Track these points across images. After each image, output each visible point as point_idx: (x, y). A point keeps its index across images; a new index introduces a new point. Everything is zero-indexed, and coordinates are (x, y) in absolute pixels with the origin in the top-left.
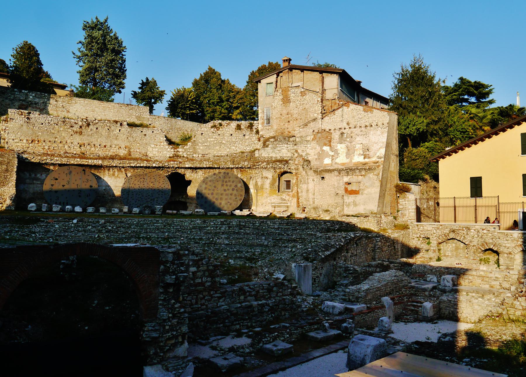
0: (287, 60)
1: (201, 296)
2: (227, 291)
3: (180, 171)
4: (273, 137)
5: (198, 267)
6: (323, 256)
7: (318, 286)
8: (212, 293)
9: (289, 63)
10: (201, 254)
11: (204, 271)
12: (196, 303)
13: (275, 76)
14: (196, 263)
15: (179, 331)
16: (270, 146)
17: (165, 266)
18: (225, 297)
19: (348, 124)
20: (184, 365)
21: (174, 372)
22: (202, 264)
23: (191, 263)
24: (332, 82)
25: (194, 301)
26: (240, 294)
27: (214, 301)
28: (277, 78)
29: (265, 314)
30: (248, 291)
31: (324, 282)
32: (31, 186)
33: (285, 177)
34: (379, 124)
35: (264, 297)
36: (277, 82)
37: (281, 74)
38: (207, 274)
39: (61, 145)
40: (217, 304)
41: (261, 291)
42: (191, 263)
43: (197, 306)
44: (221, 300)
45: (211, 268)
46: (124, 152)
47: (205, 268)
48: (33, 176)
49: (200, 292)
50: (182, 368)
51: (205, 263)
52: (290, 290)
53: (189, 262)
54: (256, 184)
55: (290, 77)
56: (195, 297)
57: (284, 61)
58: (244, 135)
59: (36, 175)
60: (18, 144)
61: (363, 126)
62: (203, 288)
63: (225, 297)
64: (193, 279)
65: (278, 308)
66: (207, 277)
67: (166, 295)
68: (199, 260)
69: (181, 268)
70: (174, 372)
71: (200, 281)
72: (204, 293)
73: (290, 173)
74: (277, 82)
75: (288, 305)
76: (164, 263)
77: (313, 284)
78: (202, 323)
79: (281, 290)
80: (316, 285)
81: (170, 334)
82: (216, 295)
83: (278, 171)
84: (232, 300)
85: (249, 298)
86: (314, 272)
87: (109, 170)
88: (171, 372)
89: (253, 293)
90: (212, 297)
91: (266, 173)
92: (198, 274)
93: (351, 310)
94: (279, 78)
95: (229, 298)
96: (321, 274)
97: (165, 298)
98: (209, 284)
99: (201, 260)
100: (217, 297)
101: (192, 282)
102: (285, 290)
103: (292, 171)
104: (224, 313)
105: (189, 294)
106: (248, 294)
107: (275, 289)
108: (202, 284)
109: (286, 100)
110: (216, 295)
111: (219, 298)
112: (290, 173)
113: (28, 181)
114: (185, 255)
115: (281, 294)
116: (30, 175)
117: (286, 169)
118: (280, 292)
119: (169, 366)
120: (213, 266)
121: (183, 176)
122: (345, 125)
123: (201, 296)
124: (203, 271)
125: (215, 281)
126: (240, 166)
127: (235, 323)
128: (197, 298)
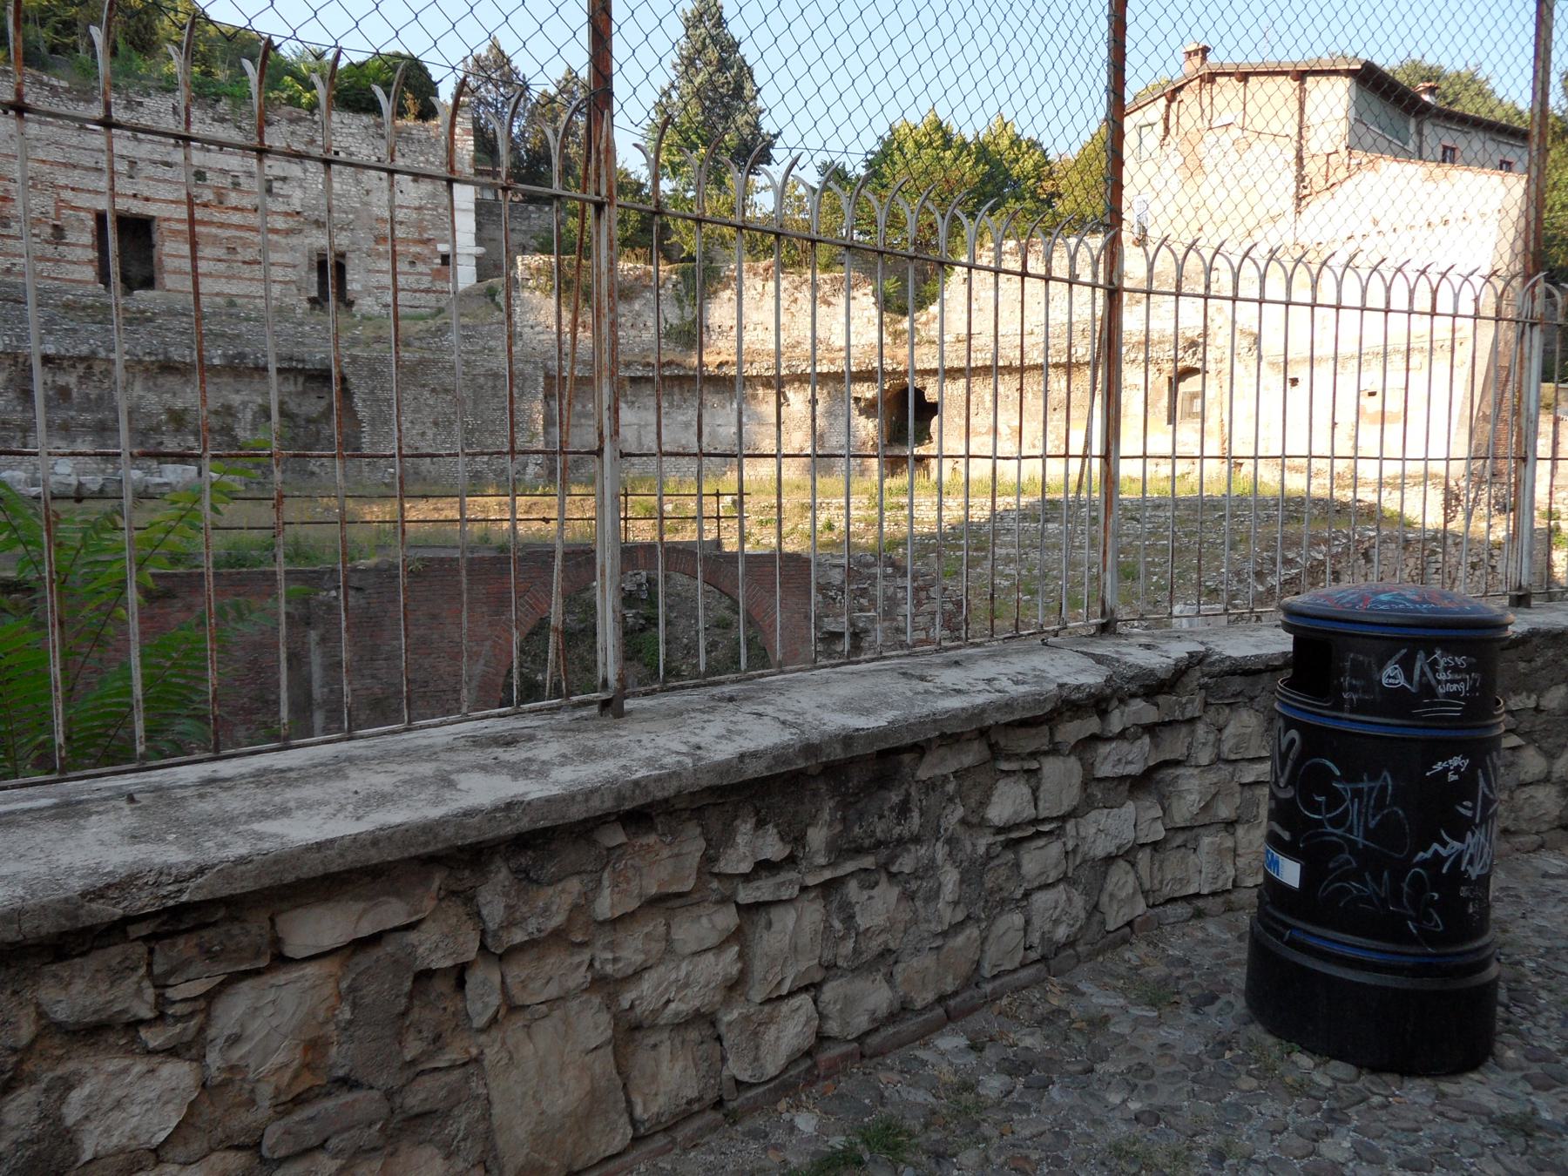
0: (1196, 52)
6: (1260, 588)
9: (1204, 58)
10: (923, 575)
13: (1163, 102)
19: (1376, 223)
22: (928, 598)
24: (1333, 100)
28: (1168, 107)
33: (1190, 385)
34: (1471, 214)
36: (1167, 119)
39: (633, 333)
48: (579, 407)
53: (895, 593)
55: (1206, 100)
57: (1189, 54)
60: (542, 337)
61: (1421, 220)
94: (1174, 106)
109: (1194, 168)
122: (1368, 227)
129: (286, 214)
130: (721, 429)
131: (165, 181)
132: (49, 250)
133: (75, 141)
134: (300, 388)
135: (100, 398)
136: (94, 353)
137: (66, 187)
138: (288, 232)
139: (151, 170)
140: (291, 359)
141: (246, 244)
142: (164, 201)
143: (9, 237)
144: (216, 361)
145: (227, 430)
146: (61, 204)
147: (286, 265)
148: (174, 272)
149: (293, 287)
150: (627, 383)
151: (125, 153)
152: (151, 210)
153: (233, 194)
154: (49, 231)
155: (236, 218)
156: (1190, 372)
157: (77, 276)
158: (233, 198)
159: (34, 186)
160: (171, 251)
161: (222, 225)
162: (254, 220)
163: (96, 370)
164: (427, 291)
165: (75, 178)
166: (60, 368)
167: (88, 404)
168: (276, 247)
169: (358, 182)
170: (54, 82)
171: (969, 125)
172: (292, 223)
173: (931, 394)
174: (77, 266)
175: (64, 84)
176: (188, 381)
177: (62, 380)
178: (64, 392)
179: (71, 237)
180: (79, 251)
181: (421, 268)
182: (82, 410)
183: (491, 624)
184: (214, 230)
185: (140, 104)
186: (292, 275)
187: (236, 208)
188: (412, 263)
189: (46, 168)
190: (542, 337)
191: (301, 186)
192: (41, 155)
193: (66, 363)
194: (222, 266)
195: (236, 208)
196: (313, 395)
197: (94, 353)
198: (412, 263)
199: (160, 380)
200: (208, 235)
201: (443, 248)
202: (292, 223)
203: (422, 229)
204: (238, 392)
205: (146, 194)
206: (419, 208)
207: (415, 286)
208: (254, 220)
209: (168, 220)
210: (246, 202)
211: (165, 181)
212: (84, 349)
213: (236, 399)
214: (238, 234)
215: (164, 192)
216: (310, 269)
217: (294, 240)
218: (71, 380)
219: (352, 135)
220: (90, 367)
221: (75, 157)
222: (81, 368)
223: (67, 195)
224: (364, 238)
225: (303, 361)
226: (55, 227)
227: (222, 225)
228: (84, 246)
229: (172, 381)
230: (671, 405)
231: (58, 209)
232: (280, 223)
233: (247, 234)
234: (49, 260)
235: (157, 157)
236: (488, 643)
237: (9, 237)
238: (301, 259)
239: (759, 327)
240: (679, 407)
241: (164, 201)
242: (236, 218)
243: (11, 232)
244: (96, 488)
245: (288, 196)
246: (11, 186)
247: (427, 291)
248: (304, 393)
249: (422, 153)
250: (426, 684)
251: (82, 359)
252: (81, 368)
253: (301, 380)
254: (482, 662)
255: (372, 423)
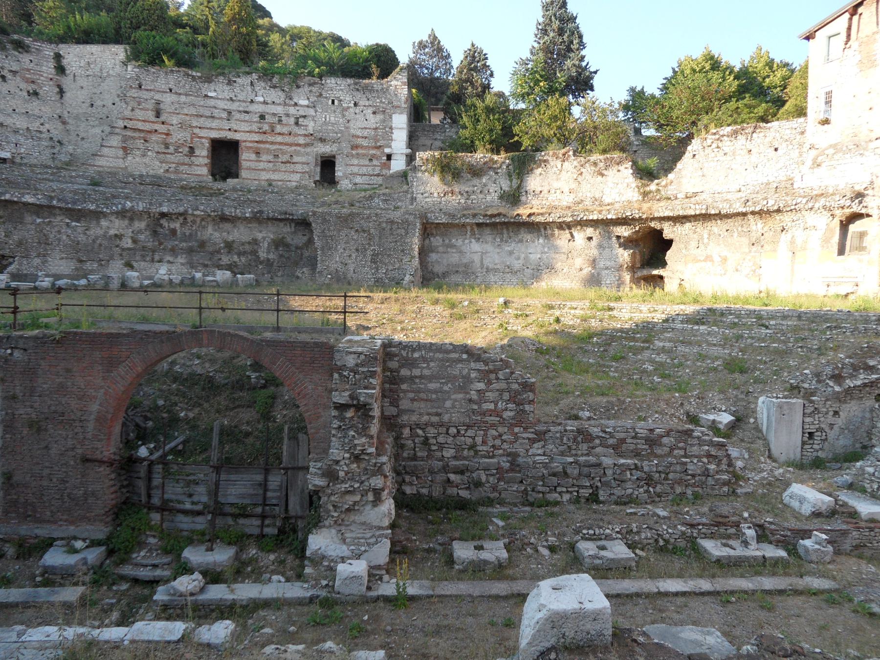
1: (494, 433)
2: (549, 431)
3: (652, 224)
4: (834, 146)
5: (489, 383)
6: (837, 389)
7: (821, 449)
8: (516, 430)
11: (501, 391)
12: (484, 442)
14: (485, 376)
15: (367, 484)
16: (823, 165)
17: (341, 375)
18: (545, 441)
20: (373, 540)
21: (353, 547)
22: (497, 379)
23: (473, 375)
25: (479, 440)
26: (579, 439)
27: (521, 444)
28: (851, 19)
29: (629, 485)
30: (598, 437)
31: (841, 442)
32: (444, 255)
35: (637, 454)
36: (849, 29)
37: (860, 10)
38: (506, 396)
39: (481, 196)
40: (527, 451)
41: (628, 441)
42: (473, 375)
43: (485, 448)
44: (535, 445)
45: (515, 386)
46: (567, 198)
47: (503, 385)
48: (447, 241)
49: (493, 426)
50: (369, 544)
51: (501, 377)
52: (707, 448)
54: (792, 242)
56: (482, 432)
58: (776, 150)
59: (450, 241)
60: (427, 200)
62: (498, 419)
63: (545, 441)
64: (479, 403)
65: (666, 479)
66: (508, 401)
67: (341, 421)
68: (491, 372)
69: (371, 380)
70: (353, 547)
71: (492, 406)
72: (500, 429)
73: (868, 216)
74: (849, 29)
75: (693, 476)
76: (340, 369)
77: (804, 443)
78: (491, 479)
79: (681, 445)
80: (815, 447)
81: (347, 486)
82: (525, 435)
83: (838, 213)
84: (561, 448)
85: (599, 450)
86: (808, 420)
87: (545, 229)
88: (349, 545)
89: (611, 441)
90: (517, 439)
91: (811, 218)
92: (487, 394)
93: (853, 514)
94: (856, 18)
95: (554, 443)
96: (831, 426)
97: (340, 427)
98: (512, 414)
99: (495, 371)
100: (529, 439)
101: (475, 407)
102: (692, 445)
103: (870, 212)
104: (535, 468)
105: (469, 427)
106: (597, 441)
107: (665, 440)
108: (497, 413)
110: (525, 435)
111: (532, 441)
112: (868, 216)
113: (441, 249)
114: (460, 361)
115: (682, 452)
116: (443, 241)
117: (856, 208)
118: (680, 449)
119: (347, 535)
120: (519, 384)
121: (660, 232)
123: (494, 433)
124: (498, 390)
125: (523, 411)
126: (757, 209)
127: (559, 489)
128: (485, 435)
129: (305, 135)
130: (531, 256)
131: (245, 121)
132: (187, 160)
133: (202, 103)
134: (293, 229)
135: (191, 235)
136: (186, 211)
137: (196, 127)
138: (306, 145)
139: (238, 116)
140: (286, 213)
141: (284, 153)
142: (244, 132)
143: (168, 153)
144: (247, 215)
145: (254, 253)
146: (194, 135)
147: (303, 163)
148: (247, 169)
149: (307, 176)
150: (475, 227)
151: (226, 107)
152: (237, 136)
153: (278, 126)
154: (187, 149)
155: (279, 139)
156: (855, 217)
157: (199, 173)
158: (279, 129)
159: (181, 127)
160: (246, 157)
161: (272, 143)
162: (288, 139)
163: (189, 220)
164: (378, 175)
165: (202, 122)
166: (171, 219)
167: (185, 238)
168: (298, 153)
169: (344, 116)
170: (194, 74)
171: (736, 55)
172: (308, 140)
173: (667, 234)
174: (200, 167)
175: (199, 74)
176: (235, 226)
177: (172, 226)
178: (173, 232)
179: (197, 153)
180: (201, 159)
181: (375, 162)
182: (181, 241)
183: (104, 379)
184: (267, 146)
185: (235, 82)
186: (306, 168)
187: (279, 134)
188: (371, 160)
189: (188, 118)
190: (427, 200)
191: (313, 120)
192: (186, 111)
193: (174, 217)
194: (271, 165)
195: (279, 134)
196: (300, 234)
197: (186, 211)
198: (371, 160)
199: (221, 226)
200: (265, 149)
201: (387, 151)
202: (308, 140)
203: (377, 141)
204: (261, 232)
205: (235, 128)
206: (376, 129)
207: (371, 173)
208: (288, 139)
209: (245, 141)
210: (285, 130)
211: (245, 121)
212: (181, 209)
213: (259, 236)
214: (277, 147)
215: (245, 127)
216: (316, 165)
217: (308, 150)
218: (176, 225)
219: (342, 90)
220: (185, 219)
221: (202, 111)
222: (181, 219)
223: (197, 131)
224: (345, 146)
225: (292, 215)
226: (191, 147)
227: (272, 143)
228: (203, 157)
229: (227, 226)
230: (502, 240)
231: (192, 138)
232: (301, 141)
233: (284, 147)
234: (186, 165)
235: (241, 109)
236: (102, 391)
237: (168, 153)
238: (311, 159)
239: (558, 191)
240: (506, 242)
241: (244, 132)
242: (279, 139)
243: (169, 151)
244: (177, 281)
245: (306, 126)
246: (171, 128)
247: (378, 175)
248: (295, 232)
249: (378, 98)
250: (63, 414)
251: (181, 214)
252: (181, 219)
253: (293, 225)
254: (98, 402)
255: (322, 249)
